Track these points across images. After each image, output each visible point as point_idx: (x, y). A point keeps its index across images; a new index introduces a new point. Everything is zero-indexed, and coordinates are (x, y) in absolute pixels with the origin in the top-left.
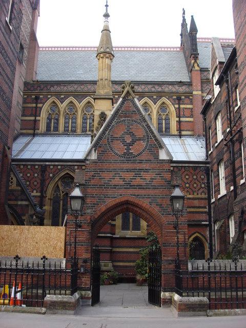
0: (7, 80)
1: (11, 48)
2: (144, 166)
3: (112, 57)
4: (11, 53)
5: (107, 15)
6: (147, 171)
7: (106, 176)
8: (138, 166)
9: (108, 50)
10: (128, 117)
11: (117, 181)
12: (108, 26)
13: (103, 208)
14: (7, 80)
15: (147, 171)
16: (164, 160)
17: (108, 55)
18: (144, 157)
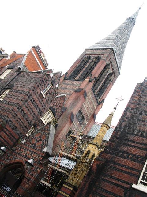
0: (33, 114)
1: (41, 104)
2: (36, 151)
3: (108, 127)
4: (41, 106)
5: (115, 108)
6: (35, 153)
7: (22, 150)
8: (34, 151)
9: (107, 123)
10: (44, 131)
11: (24, 154)
12: (113, 113)
13: (13, 161)
14: (33, 114)
15: (35, 153)
16: (44, 151)
17: (105, 125)
18: (38, 148)
